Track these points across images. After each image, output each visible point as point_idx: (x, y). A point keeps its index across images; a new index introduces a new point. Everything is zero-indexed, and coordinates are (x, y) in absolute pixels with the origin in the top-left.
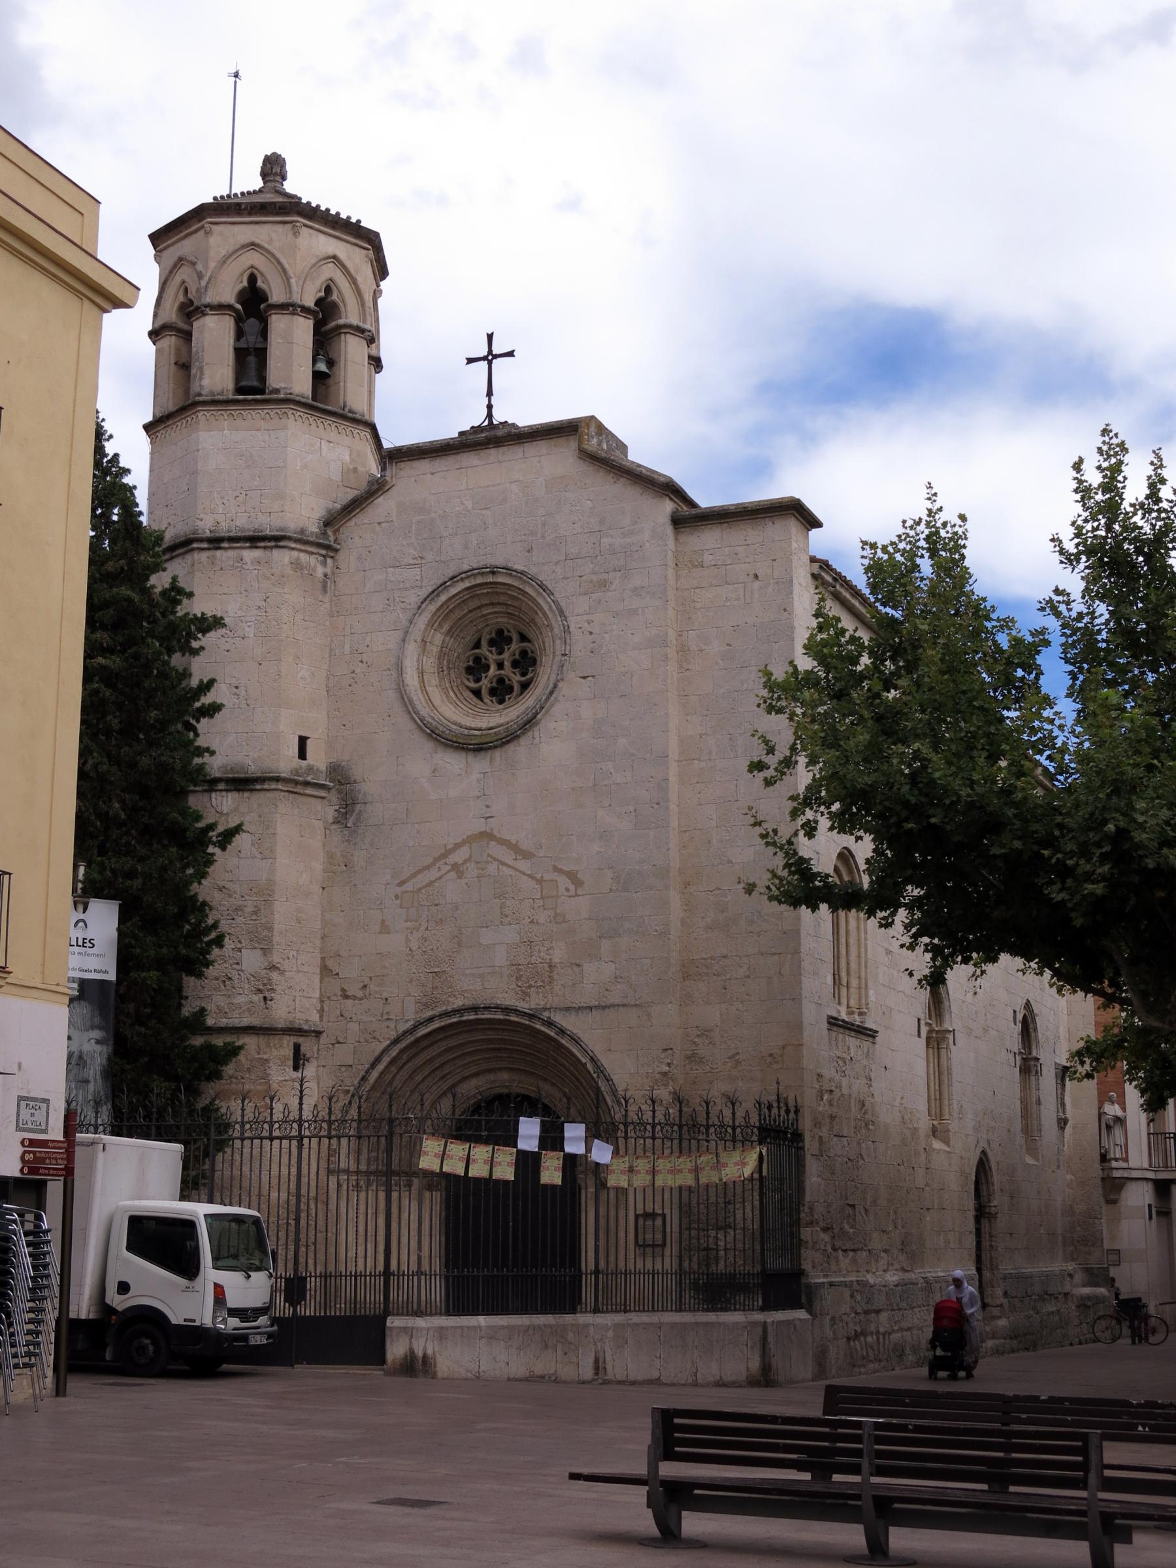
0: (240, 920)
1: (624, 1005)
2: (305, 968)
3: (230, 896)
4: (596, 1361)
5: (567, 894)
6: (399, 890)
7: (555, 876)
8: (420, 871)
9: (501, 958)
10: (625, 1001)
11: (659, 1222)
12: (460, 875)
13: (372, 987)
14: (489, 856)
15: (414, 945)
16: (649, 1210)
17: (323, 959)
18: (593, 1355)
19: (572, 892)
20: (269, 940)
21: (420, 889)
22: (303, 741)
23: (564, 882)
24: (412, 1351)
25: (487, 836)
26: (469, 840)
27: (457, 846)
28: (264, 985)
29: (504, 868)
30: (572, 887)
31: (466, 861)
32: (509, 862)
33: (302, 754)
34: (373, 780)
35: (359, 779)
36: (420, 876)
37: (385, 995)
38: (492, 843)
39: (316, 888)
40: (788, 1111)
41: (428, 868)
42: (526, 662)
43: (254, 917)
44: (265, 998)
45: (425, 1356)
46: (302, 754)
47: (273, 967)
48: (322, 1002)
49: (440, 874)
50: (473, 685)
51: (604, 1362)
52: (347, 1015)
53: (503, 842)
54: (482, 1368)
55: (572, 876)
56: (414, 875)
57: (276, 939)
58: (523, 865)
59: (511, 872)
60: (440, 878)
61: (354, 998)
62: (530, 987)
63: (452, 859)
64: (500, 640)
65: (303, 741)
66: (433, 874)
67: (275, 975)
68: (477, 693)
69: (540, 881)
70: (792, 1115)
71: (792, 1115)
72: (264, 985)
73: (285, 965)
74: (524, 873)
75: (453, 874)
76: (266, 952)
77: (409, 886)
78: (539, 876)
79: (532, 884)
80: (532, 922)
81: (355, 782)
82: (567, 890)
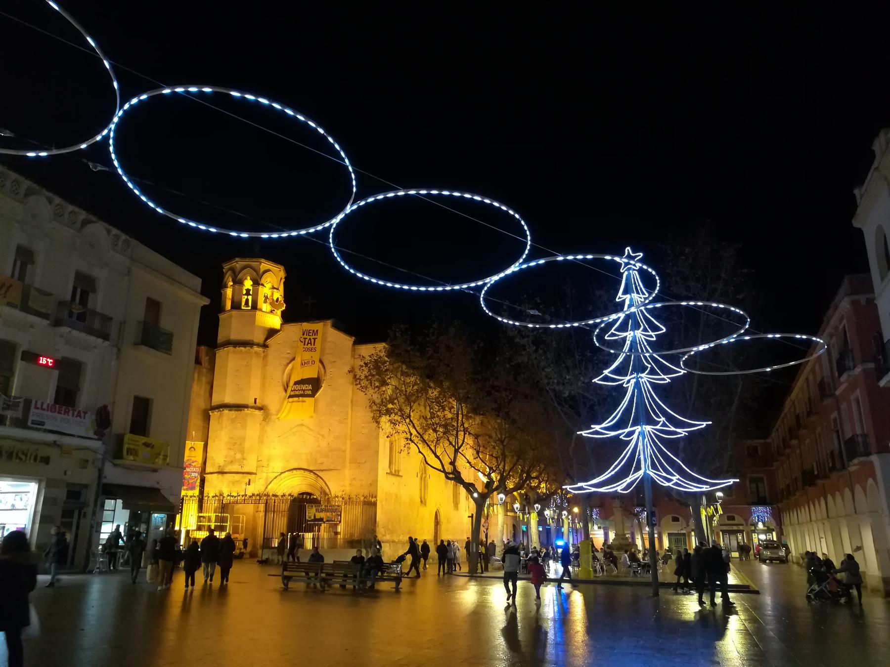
22: (255, 400)
25: (302, 425)
33: (255, 402)
46: (255, 402)
55: (323, 436)
58: (311, 432)
65: (255, 400)
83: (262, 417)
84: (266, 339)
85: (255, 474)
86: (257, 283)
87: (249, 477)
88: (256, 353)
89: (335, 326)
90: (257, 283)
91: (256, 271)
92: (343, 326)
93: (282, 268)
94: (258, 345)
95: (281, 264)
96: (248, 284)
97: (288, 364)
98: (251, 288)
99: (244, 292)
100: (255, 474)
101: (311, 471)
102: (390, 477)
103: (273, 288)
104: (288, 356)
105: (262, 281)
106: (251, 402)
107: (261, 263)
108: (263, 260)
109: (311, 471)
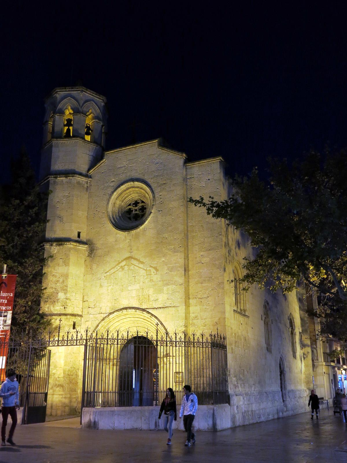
0: (58, 284)
1: (170, 307)
2: (78, 299)
3: (56, 277)
4: (156, 423)
5: (154, 274)
6: (105, 275)
7: (151, 268)
8: (112, 269)
9: (134, 294)
10: (171, 306)
11: (181, 375)
12: (123, 269)
13: (97, 304)
14: (131, 263)
15: (109, 291)
16: (177, 371)
17: (83, 296)
18: (155, 420)
19: (155, 273)
20: (66, 290)
21: (111, 274)
23: (153, 270)
24: (90, 419)
26: (126, 259)
27: (122, 261)
28: (65, 303)
29: (135, 267)
30: (155, 272)
31: (124, 266)
32: (137, 265)
34: (99, 243)
35: (95, 243)
36: (112, 270)
37: (101, 306)
38: (132, 260)
39: (82, 275)
40: (221, 338)
41: (114, 268)
42: (143, 209)
43: (62, 283)
44: (65, 308)
45: (95, 422)
47: (67, 299)
48: (83, 309)
49: (118, 269)
50: (129, 216)
51: (159, 423)
52: (90, 313)
54: (115, 425)
57: (68, 290)
58: (141, 266)
59: (137, 268)
60: (117, 270)
61: (92, 308)
62: (143, 302)
63: (120, 265)
64: (136, 203)
66: (115, 269)
67: (68, 301)
68: (130, 218)
69: (146, 270)
70: (222, 340)
71: (222, 340)
72: (65, 303)
73: (71, 298)
74: (141, 268)
75: (121, 269)
76: (65, 293)
77: (108, 274)
78: (146, 269)
79: (144, 271)
80: (143, 283)
81: (94, 244)
83: (87, 253)
84: (89, 170)
85: (81, 316)
87: (73, 319)
88: (78, 183)
89: (163, 145)
92: (169, 143)
94: (81, 174)
97: (113, 192)
98: (71, 117)
100: (81, 316)
101: (143, 310)
102: (237, 316)
104: (112, 184)
109: (143, 310)
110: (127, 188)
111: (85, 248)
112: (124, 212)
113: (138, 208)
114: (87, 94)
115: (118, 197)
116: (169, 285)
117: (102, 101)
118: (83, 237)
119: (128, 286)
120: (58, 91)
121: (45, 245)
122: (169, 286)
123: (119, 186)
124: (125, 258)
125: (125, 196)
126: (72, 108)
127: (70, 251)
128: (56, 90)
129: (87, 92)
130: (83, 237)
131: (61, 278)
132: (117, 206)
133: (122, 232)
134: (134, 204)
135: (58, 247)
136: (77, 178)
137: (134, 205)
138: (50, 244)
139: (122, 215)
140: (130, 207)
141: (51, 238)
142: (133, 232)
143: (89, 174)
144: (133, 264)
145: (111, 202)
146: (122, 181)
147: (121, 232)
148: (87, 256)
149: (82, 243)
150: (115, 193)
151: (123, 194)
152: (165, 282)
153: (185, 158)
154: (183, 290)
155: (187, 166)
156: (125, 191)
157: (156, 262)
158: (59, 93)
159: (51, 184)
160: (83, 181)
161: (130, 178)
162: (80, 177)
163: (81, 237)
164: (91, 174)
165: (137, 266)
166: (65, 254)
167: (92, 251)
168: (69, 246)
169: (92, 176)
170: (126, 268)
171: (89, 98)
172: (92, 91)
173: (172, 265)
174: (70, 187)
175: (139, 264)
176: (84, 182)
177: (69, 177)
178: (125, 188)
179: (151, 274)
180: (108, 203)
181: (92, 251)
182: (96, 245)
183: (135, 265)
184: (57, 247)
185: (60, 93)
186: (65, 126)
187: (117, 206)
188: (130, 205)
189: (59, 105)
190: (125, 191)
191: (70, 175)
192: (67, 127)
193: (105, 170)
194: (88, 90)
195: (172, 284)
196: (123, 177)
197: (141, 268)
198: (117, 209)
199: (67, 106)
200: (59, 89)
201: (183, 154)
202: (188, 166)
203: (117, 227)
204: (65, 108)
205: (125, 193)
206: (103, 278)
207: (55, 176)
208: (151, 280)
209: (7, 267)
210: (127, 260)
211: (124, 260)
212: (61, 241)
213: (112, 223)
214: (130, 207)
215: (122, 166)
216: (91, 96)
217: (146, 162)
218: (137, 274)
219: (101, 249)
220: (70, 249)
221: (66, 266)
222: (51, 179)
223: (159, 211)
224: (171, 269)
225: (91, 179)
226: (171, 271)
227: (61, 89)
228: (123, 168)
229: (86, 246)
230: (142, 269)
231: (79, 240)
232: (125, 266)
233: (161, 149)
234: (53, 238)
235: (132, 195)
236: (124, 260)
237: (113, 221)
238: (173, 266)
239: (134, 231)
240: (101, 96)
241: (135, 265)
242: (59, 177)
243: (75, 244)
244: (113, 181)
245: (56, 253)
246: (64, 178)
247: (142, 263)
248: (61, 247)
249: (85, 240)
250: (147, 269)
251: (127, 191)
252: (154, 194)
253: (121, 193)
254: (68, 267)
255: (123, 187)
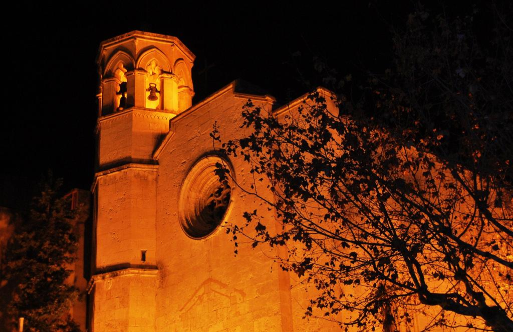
7: (236, 294)
8: (187, 303)
14: (211, 289)
23: (239, 296)
25: (210, 280)
26: (204, 283)
29: (216, 294)
31: (203, 294)
33: (144, 259)
34: (171, 265)
36: (188, 305)
38: (212, 283)
41: (190, 300)
46: (144, 259)
53: (216, 281)
55: (242, 292)
56: (185, 305)
58: (223, 291)
60: (195, 304)
66: (192, 303)
69: (229, 297)
77: (184, 311)
80: (227, 319)
82: (240, 299)
86: (130, 68)
88: (138, 176)
89: (238, 91)
90: (130, 68)
91: (129, 51)
93: (176, 41)
95: (173, 34)
96: (122, 77)
99: (119, 89)
103: (163, 72)
105: (140, 63)
106: (136, 258)
107: (135, 38)
108: (137, 33)
110: (201, 169)
111: (154, 276)
112: (205, 207)
113: (222, 198)
114: (145, 40)
115: (191, 187)
116: (260, 317)
117: (171, 44)
118: (151, 259)
119: (209, 327)
120: (105, 47)
121: (95, 278)
122: (260, 320)
123: (190, 169)
124: (204, 282)
125: (202, 182)
126: (125, 67)
127: (129, 283)
128: (102, 45)
129: (145, 36)
130: (151, 259)
131: (118, 327)
132: (193, 200)
133: (196, 241)
134: (217, 193)
135: (113, 280)
136: (135, 169)
137: (217, 195)
138: (101, 278)
139: (200, 213)
140: (212, 198)
141: (103, 267)
142: (212, 237)
143: (154, 159)
144: (213, 291)
145: (182, 196)
146: (194, 160)
147: (197, 241)
148: (158, 287)
149: (149, 268)
150: (186, 181)
151: (199, 180)
152: (255, 313)
153: (273, 102)
154: (280, 322)
155: (277, 114)
156: (200, 174)
157: (242, 282)
158: (106, 48)
159: (101, 184)
160: (145, 171)
161: (204, 152)
162: (139, 165)
163: (146, 259)
164: (158, 158)
165: (219, 293)
166: (123, 289)
167: (163, 276)
168: (127, 275)
169: (159, 161)
170: (205, 298)
171: (149, 45)
172: (150, 34)
173: (262, 283)
174: (125, 184)
175: (221, 289)
176: (146, 174)
177: (123, 169)
178: (199, 170)
179: (236, 303)
180: (179, 199)
181: (163, 276)
182: (168, 268)
183: (216, 292)
184: (112, 281)
185: (107, 48)
186: (118, 94)
187: (193, 200)
188: (212, 195)
189: (108, 65)
190: (200, 174)
191: (124, 166)
192: (121, 96)
193: (174, 148)
194: (145, 33)
195: (264, 315)
196: (195, 153)
197: (223, 295)
198: (193, 206)
199: (119, 64)
200: (106, 43)
201: (265, 97)
202: (279, 113)
203: (190, 235)
204: (115, 69)
205: (201, 177)
206: (178, 319)
207: (104, 172)
208: (238, 314)
209: (24, 321)
210: (206, 285)
211: (202, 285)
212: (114, 269)
213: (185, 228)
214: (212, 198)
215: (193, 137)
216: (128, 41)
217: (221, 123)
218: (219, 306)
219: (174, 273)
220: (130, 279)
221: (124, 308)
222: (100, 177)
223: (242, 196)
224: (262, 291)
225: (158, 166)
226: (262, 294)
227: (108, 42)
228: (195, 140)
229: (156, 271)
230: (225, 297)
231: (143, 264)
232: (204, 295)
233: (239, 97)
234: (107, 267)
235: (212, 179)
236: (202, 285)
237: (186, 225)
238: (263, 285)
239: (212, 236)
240: (168, 36)
241: (216, 292)
242: (111, 173)
243: (137, 271)
244: (184, 163)
245: (111, 290)
246: (117, 173)
247: (224, 286)
248: (117, 278)
249: (154, 263)
250: (232, 295)
251: (203, 175)
252: (234, 171)
253: (195, 179)
254: (127, 308)
255: (196, 169)
